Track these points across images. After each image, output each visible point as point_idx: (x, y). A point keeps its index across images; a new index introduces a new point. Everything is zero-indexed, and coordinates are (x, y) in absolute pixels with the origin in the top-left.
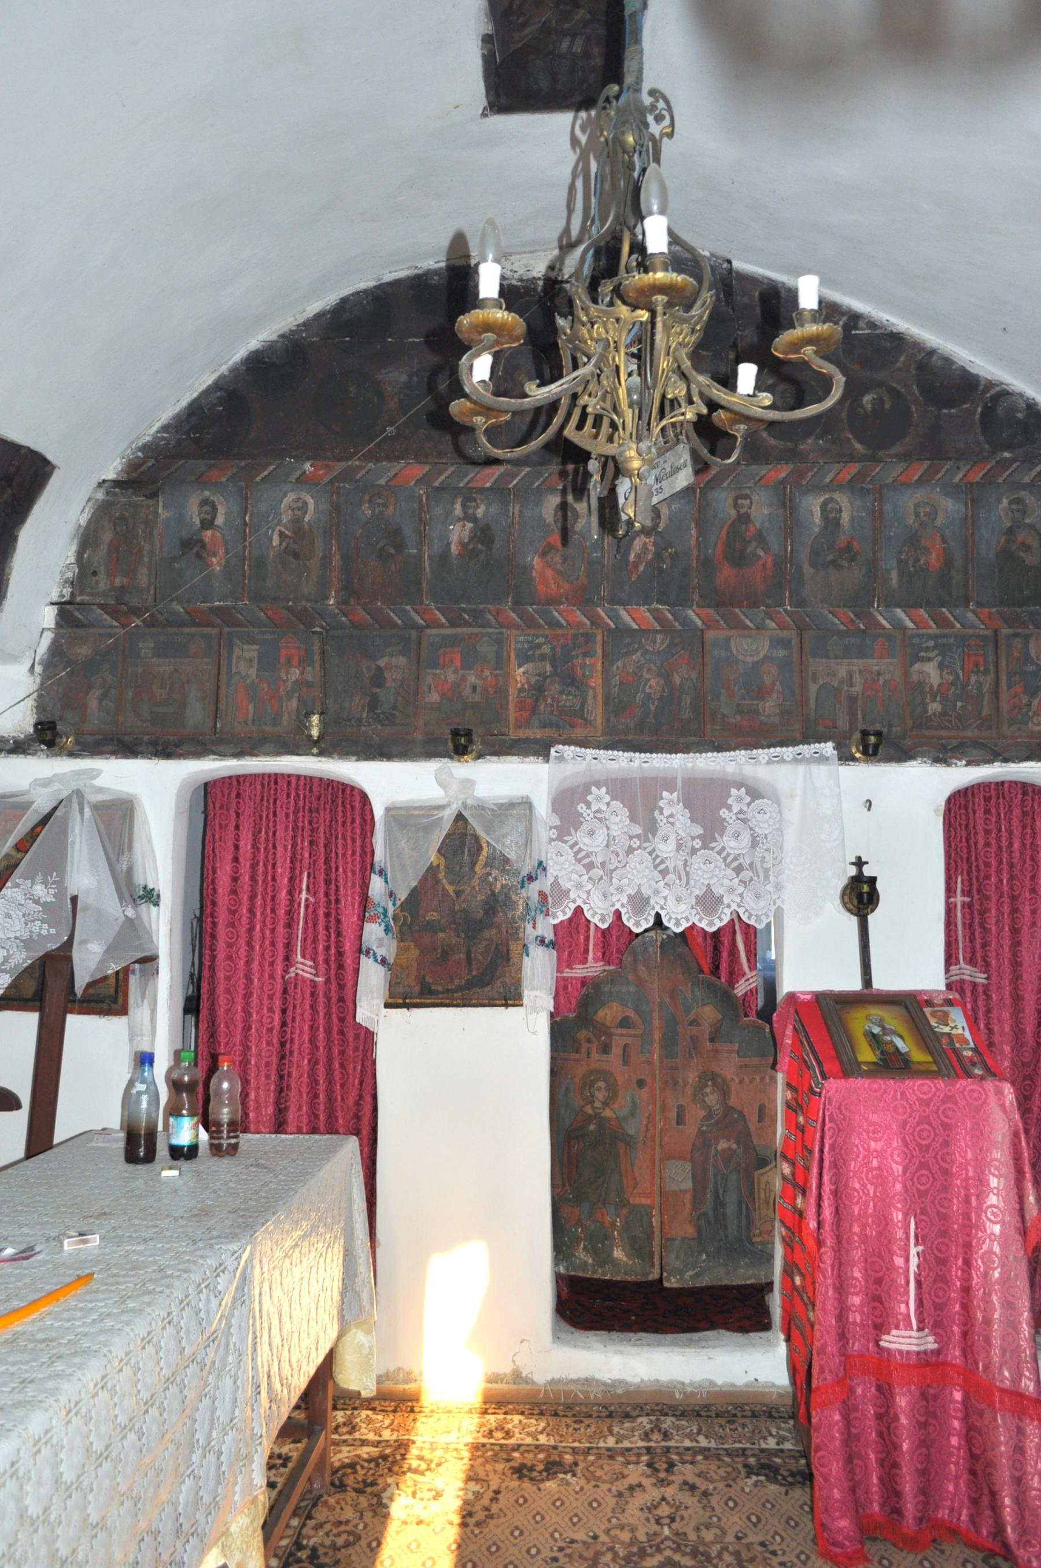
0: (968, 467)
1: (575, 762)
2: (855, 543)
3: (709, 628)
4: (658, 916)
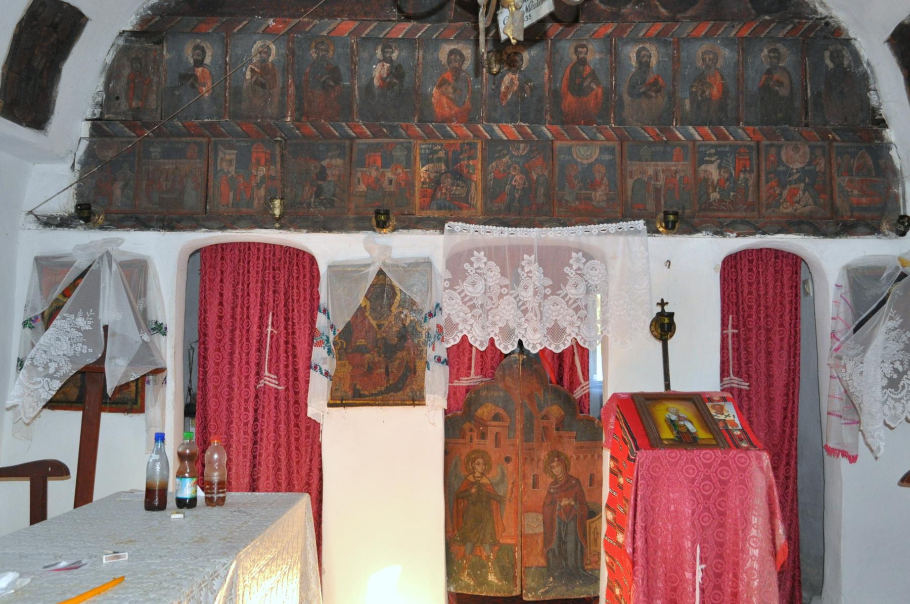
1: (462, 234)
2: (660, 80)
3: (557, 139)
4: (520, 343)
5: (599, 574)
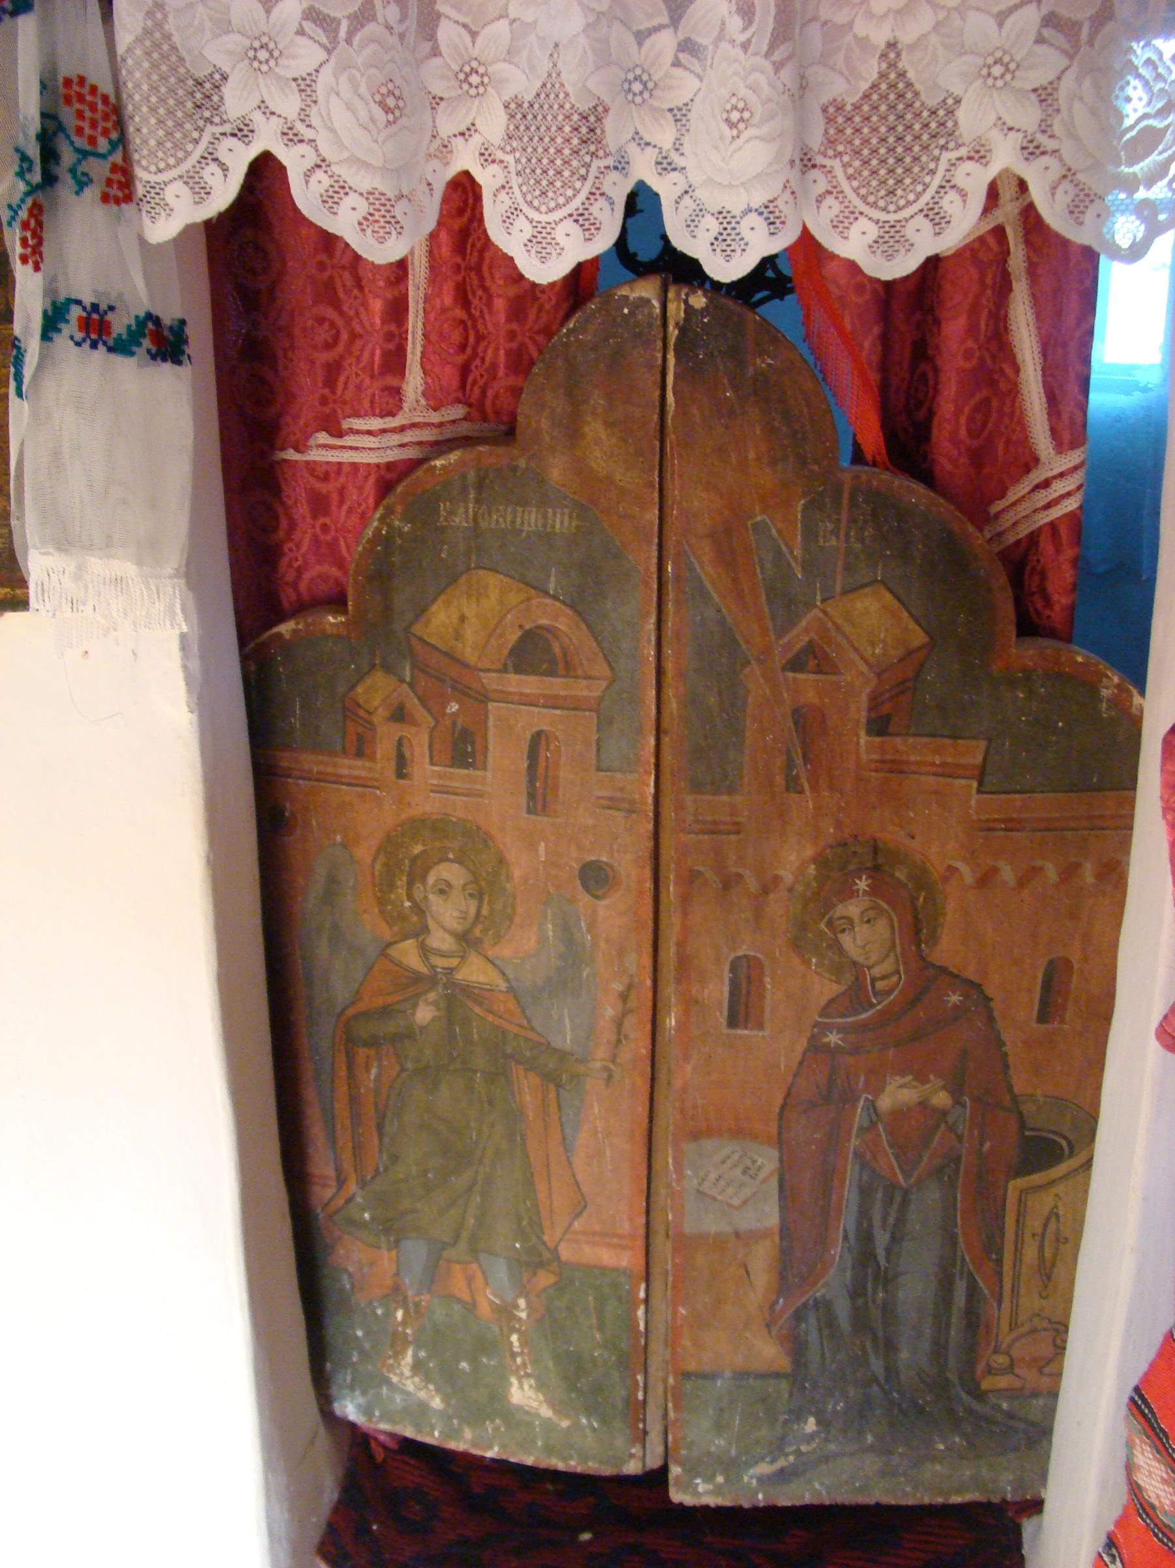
5: (1050, 1412)
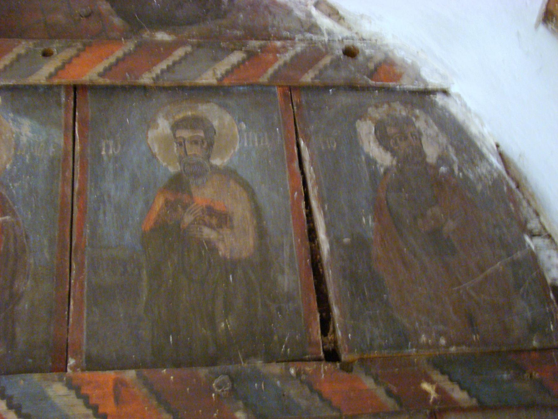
0: (72, 52)
